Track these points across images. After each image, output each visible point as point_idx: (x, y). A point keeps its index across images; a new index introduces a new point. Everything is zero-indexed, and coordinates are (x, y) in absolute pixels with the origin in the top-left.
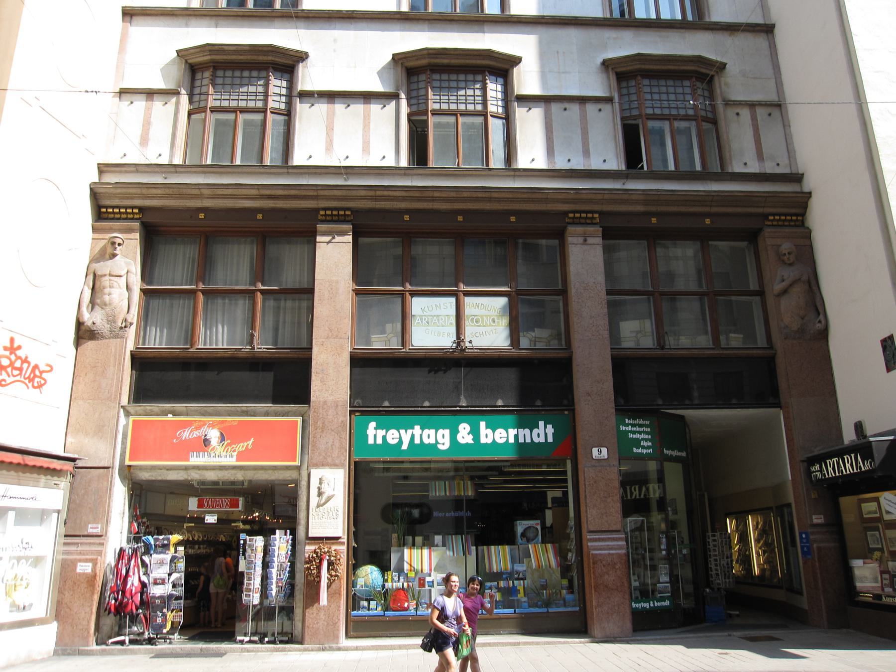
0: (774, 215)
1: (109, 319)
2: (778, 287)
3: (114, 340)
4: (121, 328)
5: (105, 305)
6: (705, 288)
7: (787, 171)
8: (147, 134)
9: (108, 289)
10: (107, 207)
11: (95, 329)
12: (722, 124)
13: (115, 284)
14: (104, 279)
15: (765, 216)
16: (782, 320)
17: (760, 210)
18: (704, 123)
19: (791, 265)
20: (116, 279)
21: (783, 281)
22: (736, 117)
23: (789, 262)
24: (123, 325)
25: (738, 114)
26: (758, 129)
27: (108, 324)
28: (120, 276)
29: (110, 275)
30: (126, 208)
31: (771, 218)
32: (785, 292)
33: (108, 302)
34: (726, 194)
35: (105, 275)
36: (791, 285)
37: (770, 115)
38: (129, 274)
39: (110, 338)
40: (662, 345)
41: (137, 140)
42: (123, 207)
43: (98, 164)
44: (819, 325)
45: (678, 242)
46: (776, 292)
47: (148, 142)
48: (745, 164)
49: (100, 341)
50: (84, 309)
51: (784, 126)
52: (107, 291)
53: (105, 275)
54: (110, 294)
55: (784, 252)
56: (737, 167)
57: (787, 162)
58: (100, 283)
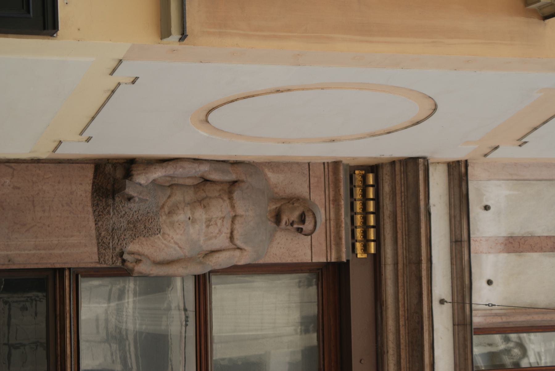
1: (138, 225)
3: (95, 241)
4: (121, 254)
5: (170, 213)
8: (532, 249)
9: (204, 217)
10: (377, 186)
11: (117, 199)
13: (214, 230)
14: (226, 205)
20: (226, 231)
24: (125, 256)
27: (129, 223)
28: (231, 238)
29: (234, 218)
30: (377, 227)
33: (175, 218)
35: (233, 207)
38: (237, 253)
39: (98, 229)
41: (518, 231)
42: (377, 220)
43: (466, 161)
47: (515, 252)
49: (90, 209)
50: (158, 174)
52: (200, 214)
53: (233, 207)
54: (192, 221)
58: (216, 197)
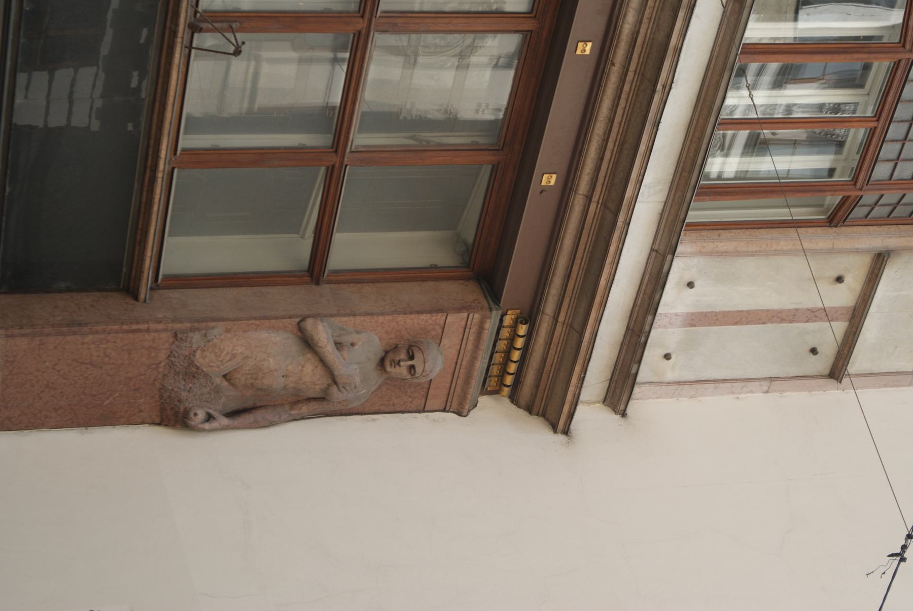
0: (529, 336)
2: (322, 333)
6: (360, 139)
7: (645, 373)
12: (822, 239)
15: (530, 317)
16: (228, 331)
17: (549, 307)
18: (838, 199)
19: (382, 363)
21: (338, 345)
22: (835, 274)
23: (387, 363)
25: (839, 279)
26: (783, 320)
31: (523, 330)
32: (308, 343)
34: (612, 249)
36: (323, 361)
37: (814, 351)
40: (204, 25)
44: (201, 415)
45: (509, 75)
46: (309, 324)
48: (690, 285)
51: (772, 379)
55: (418, 355)
56: (680, 269)
57: (670, 376)
